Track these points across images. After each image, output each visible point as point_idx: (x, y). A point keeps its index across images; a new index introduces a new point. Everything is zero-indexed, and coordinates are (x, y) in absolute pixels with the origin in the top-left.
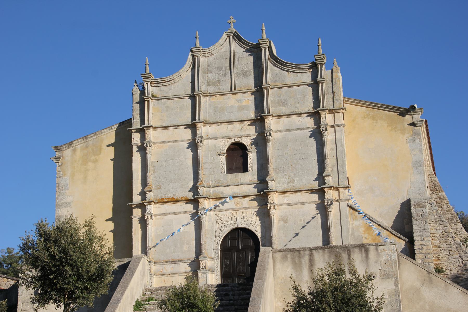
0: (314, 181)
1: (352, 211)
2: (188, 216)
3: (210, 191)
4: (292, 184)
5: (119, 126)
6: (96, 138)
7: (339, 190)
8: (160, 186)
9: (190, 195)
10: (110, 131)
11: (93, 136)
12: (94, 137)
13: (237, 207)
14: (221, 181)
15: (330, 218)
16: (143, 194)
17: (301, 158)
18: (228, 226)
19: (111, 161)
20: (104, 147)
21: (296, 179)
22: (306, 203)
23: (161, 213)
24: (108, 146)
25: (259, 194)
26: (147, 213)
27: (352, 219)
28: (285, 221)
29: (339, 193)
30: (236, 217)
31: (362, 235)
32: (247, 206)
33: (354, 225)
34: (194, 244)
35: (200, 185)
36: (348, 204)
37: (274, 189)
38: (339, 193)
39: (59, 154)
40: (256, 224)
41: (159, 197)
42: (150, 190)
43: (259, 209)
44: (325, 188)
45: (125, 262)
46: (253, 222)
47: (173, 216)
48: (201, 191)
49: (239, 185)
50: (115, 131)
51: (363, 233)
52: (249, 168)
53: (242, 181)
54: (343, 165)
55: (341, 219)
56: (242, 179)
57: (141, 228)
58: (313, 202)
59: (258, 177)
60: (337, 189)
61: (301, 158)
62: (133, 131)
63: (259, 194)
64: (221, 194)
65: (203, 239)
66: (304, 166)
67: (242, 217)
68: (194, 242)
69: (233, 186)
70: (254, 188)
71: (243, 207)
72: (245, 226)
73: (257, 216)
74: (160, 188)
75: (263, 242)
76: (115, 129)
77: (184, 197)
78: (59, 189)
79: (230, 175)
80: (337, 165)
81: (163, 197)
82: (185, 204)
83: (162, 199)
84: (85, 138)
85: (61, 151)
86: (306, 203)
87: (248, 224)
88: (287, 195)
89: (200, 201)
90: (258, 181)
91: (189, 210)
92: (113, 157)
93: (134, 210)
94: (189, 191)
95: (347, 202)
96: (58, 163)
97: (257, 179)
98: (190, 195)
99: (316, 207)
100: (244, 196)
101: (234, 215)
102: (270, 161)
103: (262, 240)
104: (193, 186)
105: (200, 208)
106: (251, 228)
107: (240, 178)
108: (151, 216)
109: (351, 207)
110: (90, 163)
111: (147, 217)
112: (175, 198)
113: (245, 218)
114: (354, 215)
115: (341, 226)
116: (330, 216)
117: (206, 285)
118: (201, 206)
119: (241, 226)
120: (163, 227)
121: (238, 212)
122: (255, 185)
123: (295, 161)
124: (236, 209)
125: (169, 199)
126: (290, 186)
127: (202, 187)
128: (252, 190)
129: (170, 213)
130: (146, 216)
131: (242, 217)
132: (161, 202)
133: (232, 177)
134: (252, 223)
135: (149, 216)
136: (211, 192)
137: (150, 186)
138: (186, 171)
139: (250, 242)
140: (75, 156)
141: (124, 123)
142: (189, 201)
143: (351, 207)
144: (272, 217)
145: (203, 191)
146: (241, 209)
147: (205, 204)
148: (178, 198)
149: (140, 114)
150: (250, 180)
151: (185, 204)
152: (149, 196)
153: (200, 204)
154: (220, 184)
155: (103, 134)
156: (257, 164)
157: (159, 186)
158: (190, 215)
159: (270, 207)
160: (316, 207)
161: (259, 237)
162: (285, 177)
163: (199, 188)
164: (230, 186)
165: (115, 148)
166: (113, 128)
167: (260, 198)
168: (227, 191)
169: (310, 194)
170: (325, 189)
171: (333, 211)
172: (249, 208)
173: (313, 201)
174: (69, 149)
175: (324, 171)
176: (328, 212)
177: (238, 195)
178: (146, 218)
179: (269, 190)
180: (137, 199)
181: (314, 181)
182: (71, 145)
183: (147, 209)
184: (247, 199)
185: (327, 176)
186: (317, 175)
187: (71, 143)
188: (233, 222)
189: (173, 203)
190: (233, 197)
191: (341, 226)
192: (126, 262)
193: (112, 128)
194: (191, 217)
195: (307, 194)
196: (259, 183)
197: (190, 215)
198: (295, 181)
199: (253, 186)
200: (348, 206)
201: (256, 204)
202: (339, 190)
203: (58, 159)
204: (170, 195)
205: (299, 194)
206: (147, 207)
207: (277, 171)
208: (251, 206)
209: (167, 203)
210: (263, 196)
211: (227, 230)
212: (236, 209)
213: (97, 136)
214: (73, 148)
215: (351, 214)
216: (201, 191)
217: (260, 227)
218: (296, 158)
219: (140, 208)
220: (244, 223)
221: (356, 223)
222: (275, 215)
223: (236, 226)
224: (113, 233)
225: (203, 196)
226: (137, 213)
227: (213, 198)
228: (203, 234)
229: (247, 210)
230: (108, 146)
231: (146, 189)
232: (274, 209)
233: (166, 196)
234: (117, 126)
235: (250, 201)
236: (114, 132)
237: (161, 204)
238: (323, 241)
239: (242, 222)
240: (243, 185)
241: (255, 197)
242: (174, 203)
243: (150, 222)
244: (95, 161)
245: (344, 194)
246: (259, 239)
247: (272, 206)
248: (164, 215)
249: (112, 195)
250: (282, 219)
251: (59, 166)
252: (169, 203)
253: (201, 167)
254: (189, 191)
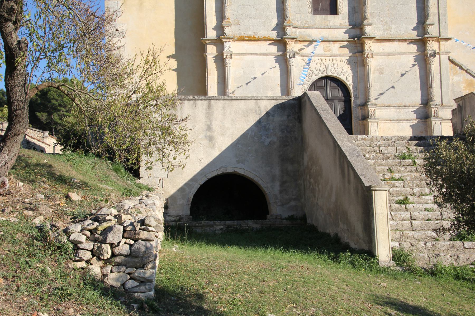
0: (413, 30)
1: (452, 65)
2: (272, 59)
3: (296, 32)
4: (388, 32)
7: (439, 42)
8: (238, 21)
9: (274, 35)
13: (326, 53)
14: (308, 22)
15: (432, 71)
16: (220, 28)
17: (399, 4)
18: (316, 73)
21: (393, 27)
22: (405, 53)
23: (240, 53)
25: (352, 40)
26: (225, 51)
27: (452, 74)
28: (381, 72)
29: (439, 45)
30: (326, 64)
31: (463, 91)
32: (338, 53)
33: (454, 80)
34: (280, 91)
35: (288, 24)
36: (449, 57)
37: (372, 35)
38: (439, 45)
40: (347, 74)
41: (238, 34)
42: (230, 24)
43: (350, 57)
44: (428, 37)
45: (283, 101)
46: (344, 70)
47: (255, 58)
48: (289, 31)
49: (328, 28)
51: (464, 90)
52: (339, 10)
53: (332, 24)
54: (445, 15)
55: (442, 73)
56: (331, 22)
57: (216, 68)
58: (411, 53)
59: (349, 22)
60: (438, 40)
61: (399, 4)
63: (352, 40)
64: (308, 37)
65: (292, 86)
66: (402, 12)
67: (332, 65)
68: (279, 88)
69: (322, 28)
70: (344, 33)
71: (333, 53)
72: (335, 74)
73: (348, 64)
74: (238, 24)
75: (355, 94)
77: (267, 36)
79: (318, 17)
80: (437, 14)
81: (242, 35)
82: (268, 45)
83: (241, 36)
86: (405, 53)
87: (339, 72)
88: (384, 43)
89: (288, 42)
90: (350, 25)
91: (273, 52)
93: (208, 46)
94: (272, 30)
95: (448, 56)
97: (348, 24)
98: (274, 35)
99: (414, 59)
100: (334, 42)
101: (323, 61)
102: (367, 4)
103: (354, 91)
104: (277, 24)
105: (288, 50)
106: (342, 77)
107: (330, 21)
108: (231, 55)
109: (452, 61)
111: (226, 56)
112: (256, 36)
113: (336, 65)
114: (455, 70)
115: (441, 81)
116: (432, 69)
117: (397, 137)
118: (289, 48)
119: (331, 74)
120: (242, 68)
121: (327, 58)
122: (346, 30)
123: (392, 6)
124: (325, 55)
125: (249, 37)
126: (387, 35)
127: (290, 26)
128: (342, 35)
129: (251, 54)
130: (225, 55)
131: (332, 65)
132: (241, 39)
133: (320, 19)
134: (344, 72)
135: (229, 54)
136: (297, 33)
137: (229, 20)
138: (268, 7)
139: (338, 93)
142: (273, 42)
143: (452, 61)
144: (369, 66)
145: (290, 31)
146: (331, 55)
147: (292, 46)
148: (260, 37)
150: (341, 24)
151: (268, 45)
152: (227, 31)
153: (288, 46)
154: (307, 26)
156: (348, 6)
157: (237, 21)
158: (274, 57)
159: (368, 55)
160: (414, 59)
161: (351, 87)
162: (381, 23)
163: (287, 27)
164: (319, 28)
167: (352, 45)
168: (314, 34)
169: (408, 44)
170: (429, 39)
171: (435, 63)
172: (340, 55)
173: (412, 52)
175: (427, 19)
176: (431, 65)
177: (329, 40)
178: (225, 57)
179: (367, 36)
180: (211, 34)
181: (413, 30)
183: (225, 47)
184: (338, 45)
185: (430, 25)
186: (416, 24)
188: (322, 69)
189: (254, 42)
190: (322, 41)
191: (441, 81)
192: (285, 101)
194: (275, 60)
195: (405, 44)
196: (351, 28)
197: (274, 57)
198: (392, 28)
199: (344, 30)
200: (449, 60)
201: (346, 51)
202: (439, 42)
204: (250, 33)
205: (396, 44)
206: (225, 44)
207: (372, 16)
208: (343, 53)
209: (248, 42)
210: (356, 43)
211: (315, 78)
212: (326, 55)
215: (451, 69)
216: (289, 31)
217: (351, 77)
218: (393, 2)
219: (215, 45)
220: (334, 71)
221: (456, 79)
222: (372, 64)
223: (325, 74)
224: (176, 73)
225: (290, 37)
226: (211, 50)
227: (300, 41)
228: (292, 80)
229: (338, 58)
231: (224, 23)
232: (372, 57)
233: (246, 33)
235: (341, 47)
237: (240, 42)
238: (421, 96)
239: (332, 70)
240: (333, 28)
241: (346, 43)
242: (256, 42)
243: (229, 62)
245: (445, 45)
246: (351, 90)
247: (370, 54)
248: (244, 56)
249: (174, 28)
250: (378, 70)
252: (250, 42)
253: (288, 3)
254: (272, 30)
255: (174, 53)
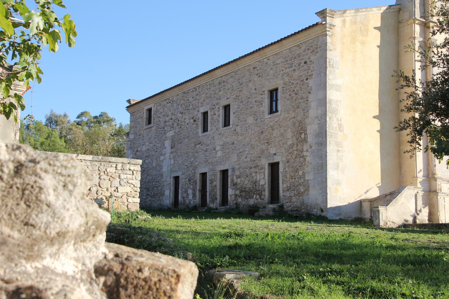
5: (387, 9)
6: (364, 15)
10: (378, 12)
11: (363, 12)
12: (364, 13)
19: (377, 47)
20: (371, 28)
24: (375, 28)
39: (330, 21)
50: (382, 13)
62: (417, 22)
76: (382, 12)
78: (329, 65)
84: (357, 10)
85: (333, 18)
92: (379, 44)
96: (329, 31)
110: (358, 44)
140: (344, 29)
141: (391, 7)
149: (419, 4)
155: (371, 13)
165: (381, 33)
166: (381, 9)
174: (339, 18)
182: (344, 13)
187: (345, 12)
193: (380, 9)
203: (332, 27)
213: (366, 13)
214: (343, 18)
230: (375, 28)
234: (385, 8)
236: (380, 15)
244: (363, 43)
251: (329, 36)
255: (378, 114)
